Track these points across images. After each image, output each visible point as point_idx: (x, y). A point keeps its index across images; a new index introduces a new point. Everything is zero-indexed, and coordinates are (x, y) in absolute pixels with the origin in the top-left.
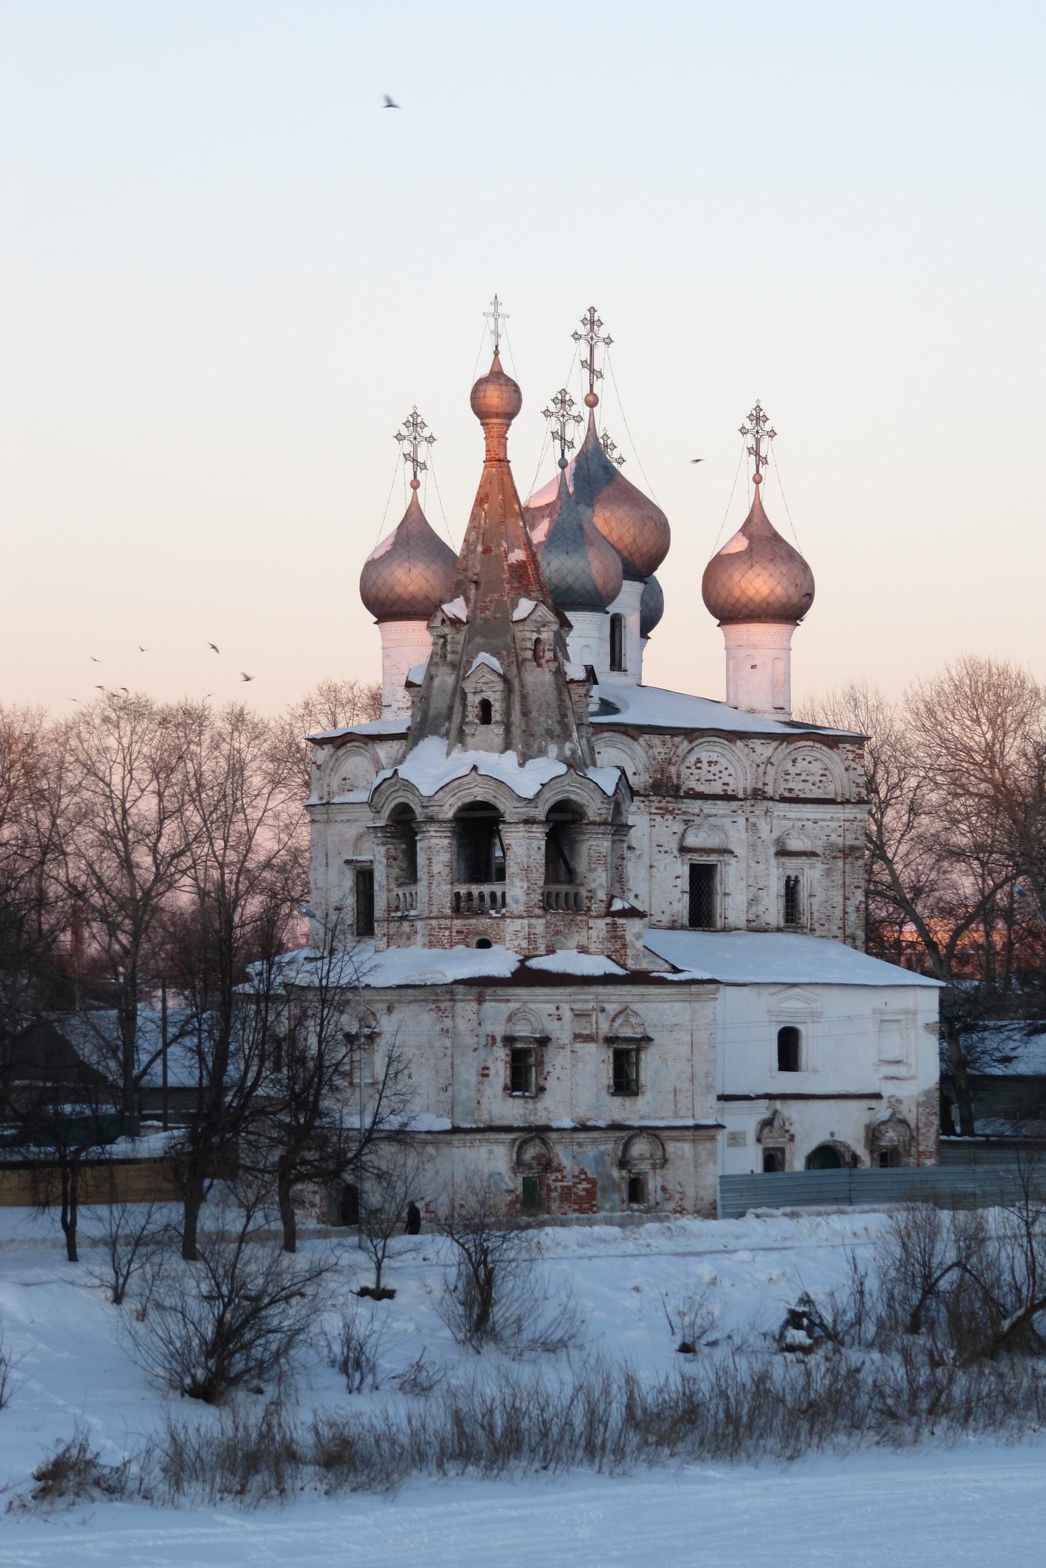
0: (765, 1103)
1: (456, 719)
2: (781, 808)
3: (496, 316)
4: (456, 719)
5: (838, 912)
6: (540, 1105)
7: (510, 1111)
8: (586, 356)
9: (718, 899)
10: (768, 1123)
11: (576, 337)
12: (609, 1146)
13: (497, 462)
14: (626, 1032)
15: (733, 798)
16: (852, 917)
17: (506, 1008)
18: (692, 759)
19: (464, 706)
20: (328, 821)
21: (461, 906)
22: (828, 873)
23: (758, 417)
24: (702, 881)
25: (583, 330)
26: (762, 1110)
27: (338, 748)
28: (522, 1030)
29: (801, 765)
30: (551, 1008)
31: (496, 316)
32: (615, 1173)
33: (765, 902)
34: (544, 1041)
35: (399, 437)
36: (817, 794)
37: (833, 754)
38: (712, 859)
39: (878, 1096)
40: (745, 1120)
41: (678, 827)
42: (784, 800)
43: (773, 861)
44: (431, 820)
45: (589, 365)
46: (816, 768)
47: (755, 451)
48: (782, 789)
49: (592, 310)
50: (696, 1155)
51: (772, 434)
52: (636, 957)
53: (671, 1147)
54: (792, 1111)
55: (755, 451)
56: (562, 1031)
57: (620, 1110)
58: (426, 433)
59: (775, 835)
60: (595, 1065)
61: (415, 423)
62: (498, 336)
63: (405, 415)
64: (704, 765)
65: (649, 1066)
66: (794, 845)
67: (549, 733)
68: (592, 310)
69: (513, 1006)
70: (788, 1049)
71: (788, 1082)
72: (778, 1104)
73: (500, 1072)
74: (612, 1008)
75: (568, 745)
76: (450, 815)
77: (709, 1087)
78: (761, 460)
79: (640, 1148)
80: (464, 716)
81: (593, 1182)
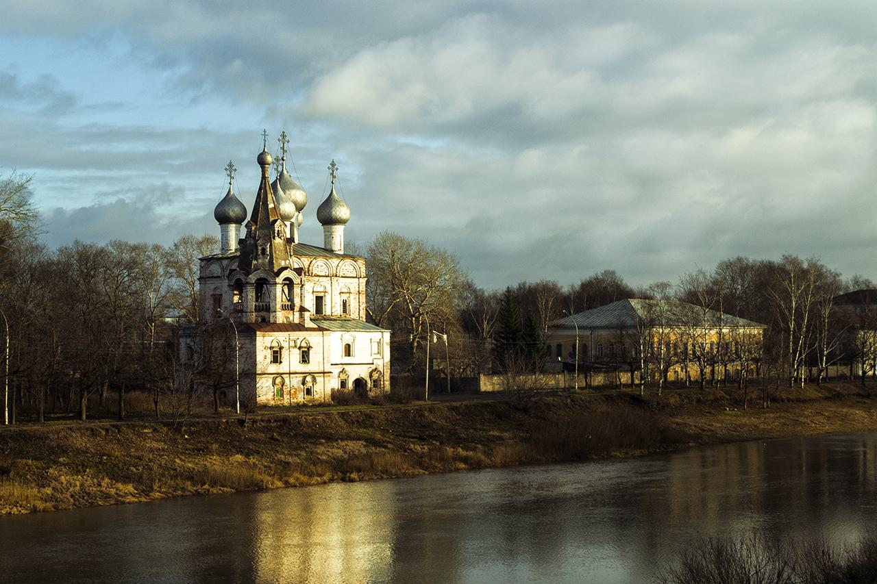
0: (341, 366)
1: (255, 254)
2: (341, 280)
3: (265, 135)
4: (255, 254)
6: (281, 367)
7: (273, 368)
8: (282, 146)
10: (343, 371)
11: (279, 140)
13: (264, 178)
14: (304, 344)
16: (361, 311)
17: (271, 338)
18: (315, 266)
19: (257, 250)
20: (205, 284)
21: (258, 309)
22: (355, 298)
23: (333, 164)
24: (319, 300)
25: (281, 138)
26: (340, 368)
27: (232, 260)
28: (275, 344)
31: (265, 135)
32: (302, 386)
34: (281, 348)
35: (226, 169)
36: (352, 275)
38: (322, 294)
40: (336, 370)
41: (313, 285)
42: (342, 277)
44: (248, 283)
45: (283, 148)
47: (332, 174)
48: (341, 274)
49: (284, 132)
51: (337, 169)
53: (318, 379)
55: (332, 174)
58: (234, 168)
60: (296, 354)
61: (231, 165)
62: (265, 141)
63: (228, 163)
64: (319, 267)
65: (312, 354)
68: (284, 132)
69: (273, 338)
70: (348, 350)
72: (344, 366)
74: (301, 339)
75: (287, 261)
76: (254, 282)
77: (328, 361)
78: (334, 177)
79: (309, 379)
80: (257, 253)
81: (296, 389)
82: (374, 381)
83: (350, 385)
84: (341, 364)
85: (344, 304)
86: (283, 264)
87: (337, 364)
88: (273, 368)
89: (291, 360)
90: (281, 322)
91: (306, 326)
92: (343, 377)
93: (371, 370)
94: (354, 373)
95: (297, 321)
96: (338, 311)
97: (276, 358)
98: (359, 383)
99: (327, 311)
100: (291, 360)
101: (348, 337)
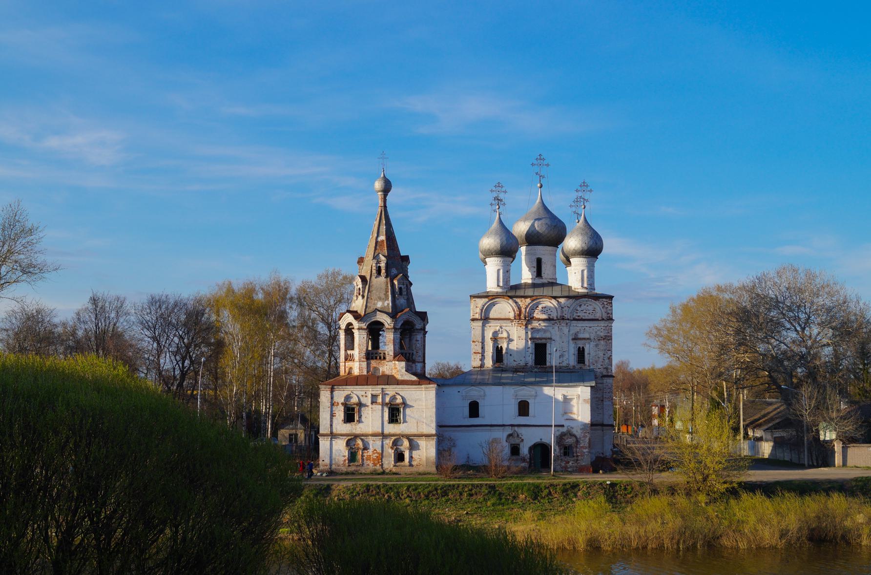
5: (601, 360)
7: (347, 428)
9: (548, 355)
12: (389, 442)
15: (553, 320)
22: (597, 345)
26: (509, 431)
29: (583, 307)
30: (363, 393)
33: (567, 356)
36: (591, 317)
37: (597, 302)
38: (543, 341)
39: (563, 426)
42: (574, 319)
43: (571, 342)
46: (590, 308)
50: (427, 445)
52: (402, 375)
54: (523, 431)
56: (367, 401)
57: (390, 429)
59: (573, 332)
66: (581, 336)
67: (380, 299)
70: (523, 408)
71: (523, 420)
72: (516, 428)
73: (340, 413)
82: (565, 448)
83: (525, 450)
84: (512, 426)
85: (581, 353)
86: (379, 305)
87: (504, 425)
88: (347, 428)
89: (372, 420)
90: (365, 373)
91: (399, 377)
92: (517, 441)
93: (558, 433)
94: (529, 438)
95: (388, 373)
96: (571, 360)
97: (350, 416)
98: (542, 449)
99: (553, 360)
100: (372, 420)
101: (525, 392)
